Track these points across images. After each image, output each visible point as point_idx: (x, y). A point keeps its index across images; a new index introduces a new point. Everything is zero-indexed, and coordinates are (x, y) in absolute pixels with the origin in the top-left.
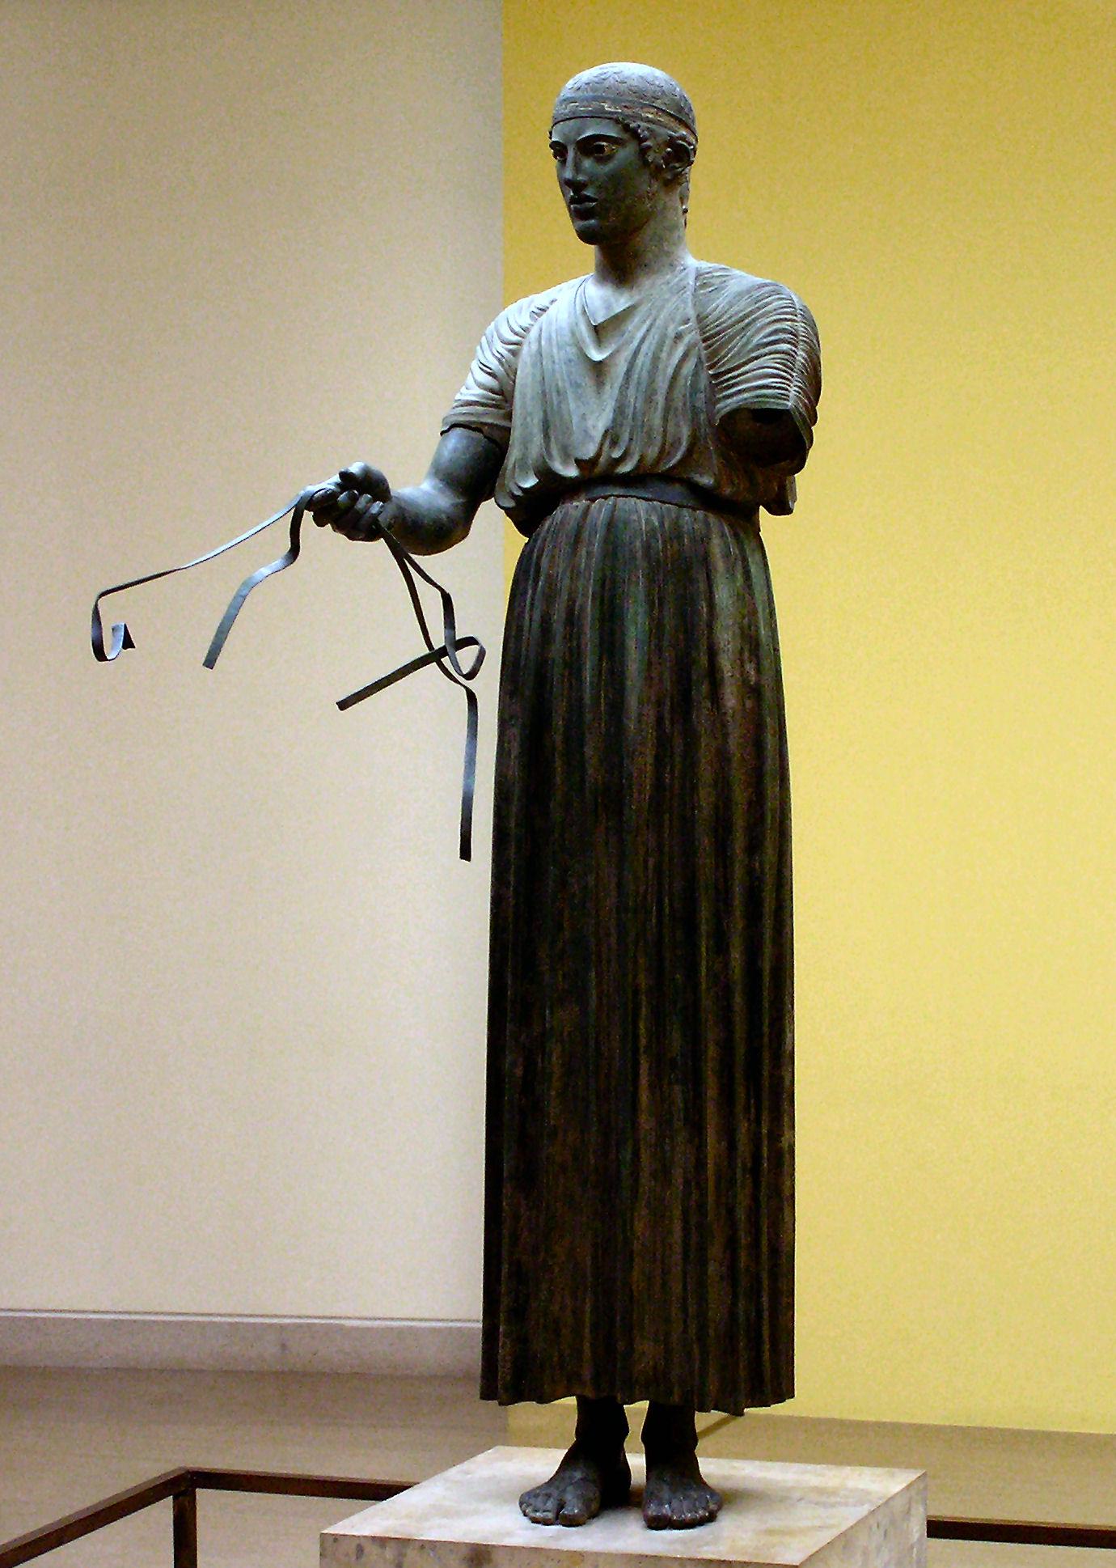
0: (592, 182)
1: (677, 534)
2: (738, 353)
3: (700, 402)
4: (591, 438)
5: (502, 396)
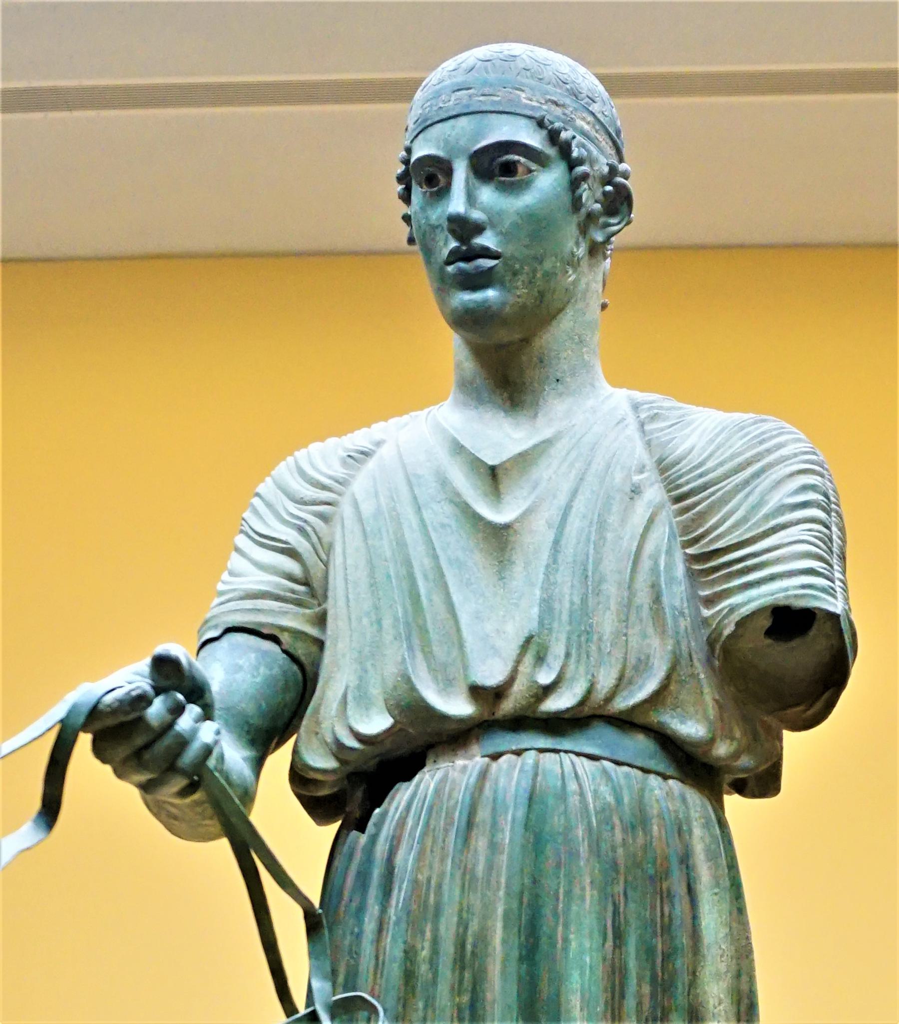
0: (493, 226)
1: (640, 820)
2: (745, 519)
3: (677, 594)
4: (496, 651)
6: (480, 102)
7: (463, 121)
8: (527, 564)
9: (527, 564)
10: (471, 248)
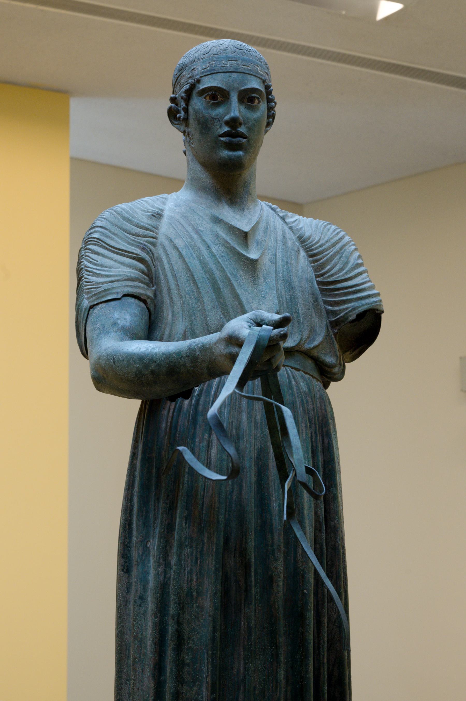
0: (245, 124)
2: (342, 269)
5: (151, 276)
6: (242, 67)
7: (235, 75)
8: (265, 279)
9: (265, 279)
10: (237, 132)
